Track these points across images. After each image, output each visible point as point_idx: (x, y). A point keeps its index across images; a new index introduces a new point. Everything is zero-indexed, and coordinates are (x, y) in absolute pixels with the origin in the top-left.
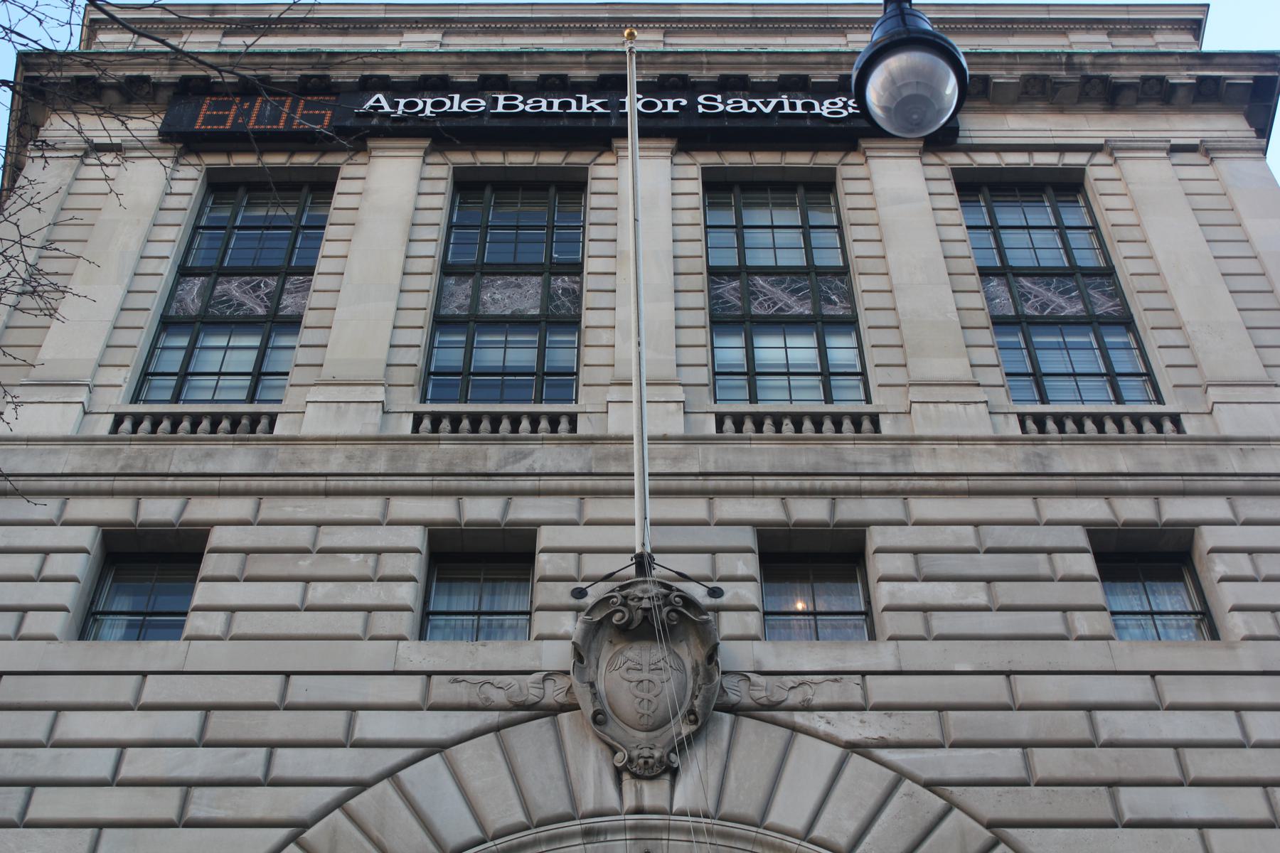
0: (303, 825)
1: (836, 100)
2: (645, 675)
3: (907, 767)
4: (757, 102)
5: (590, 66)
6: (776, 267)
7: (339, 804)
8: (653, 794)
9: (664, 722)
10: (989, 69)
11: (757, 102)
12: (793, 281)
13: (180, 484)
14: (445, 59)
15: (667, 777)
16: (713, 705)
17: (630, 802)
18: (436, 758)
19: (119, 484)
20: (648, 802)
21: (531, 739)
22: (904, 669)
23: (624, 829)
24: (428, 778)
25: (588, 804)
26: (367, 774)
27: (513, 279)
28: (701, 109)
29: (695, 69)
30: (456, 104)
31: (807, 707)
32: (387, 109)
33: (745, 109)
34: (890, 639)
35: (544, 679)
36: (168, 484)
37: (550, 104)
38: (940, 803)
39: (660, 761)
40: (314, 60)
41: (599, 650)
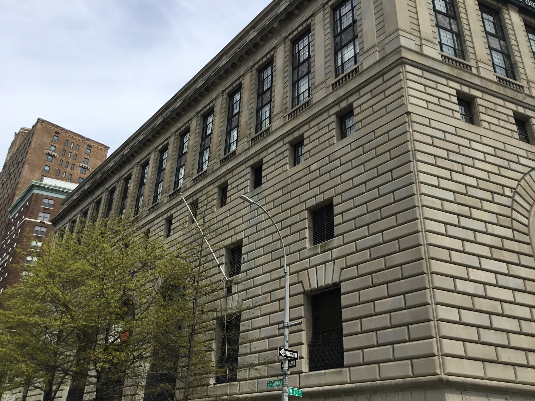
13: (468, 83)
19: (456, 79)
26: (526, 172)
36: (465, 83)
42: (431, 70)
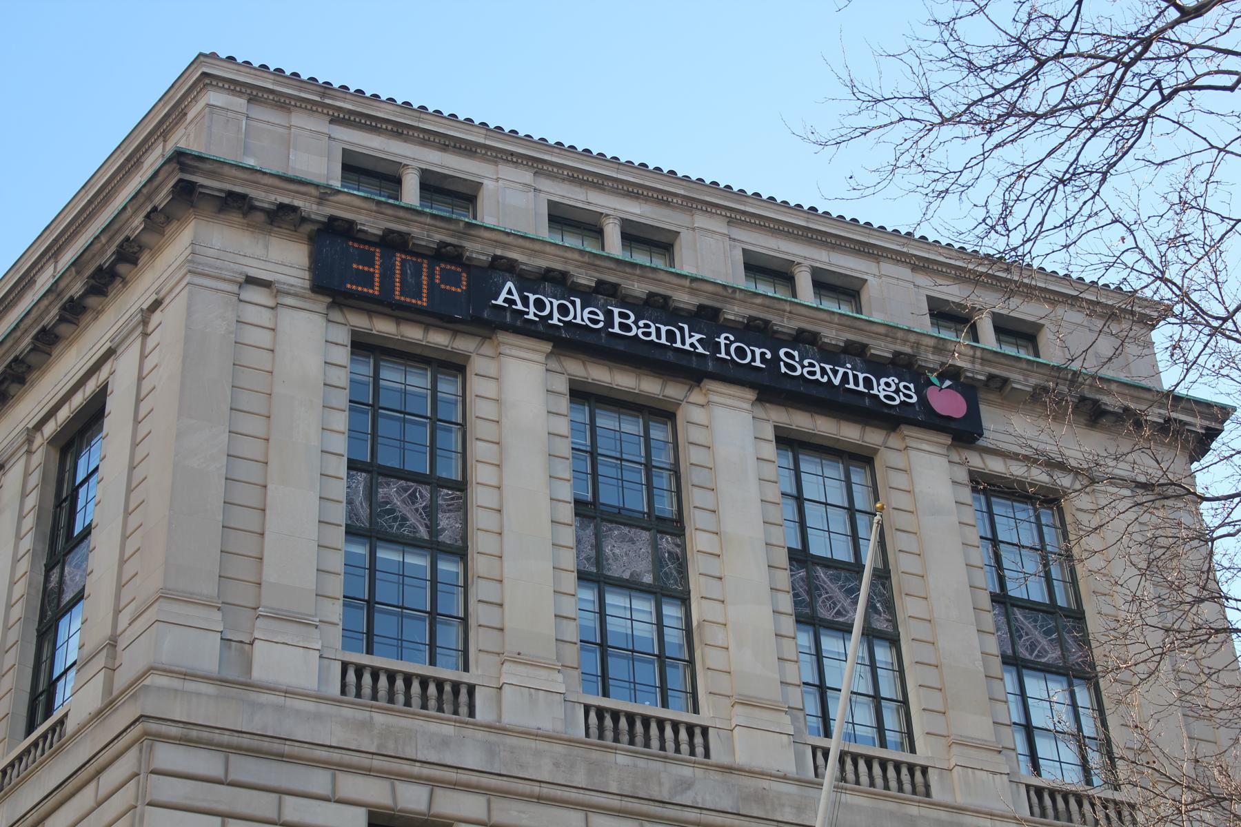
1: (890, 380)
4: (828, 367)
5: (693, 292)
6: (832, 560)
10: (1010, 371)
11: (828, 367)
12: (847, 579)
13: (427, 771)
14: (569, 255)
19: (377, 763)
27: (626, 530)
28: (783, 370)
29: (778, 315)
30: (581, 315)
32: (520, 307)
33: (818, 376)
36: (416, 769)
37: (655, 332)
40: (452, 227)
42: (266, 745)
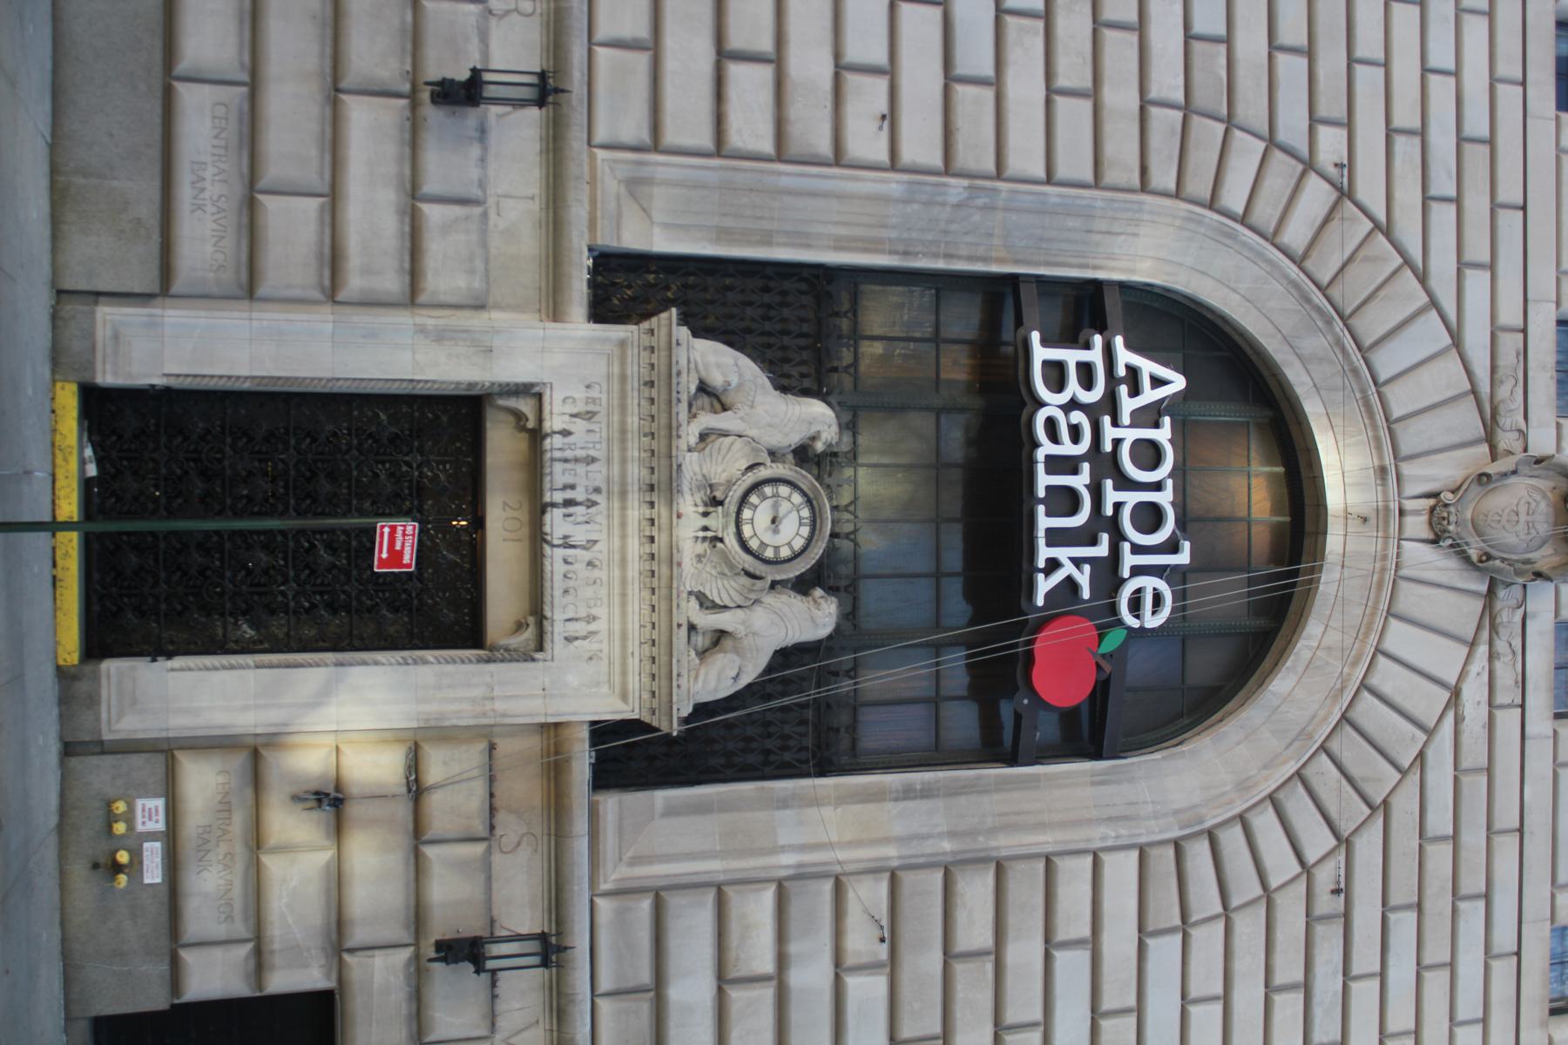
0: (1387, 231)
2: (1523, 518)
3: (1437, 738)
7: (1407, 262)
8: (1417, 525)
9: (1479, 533)
15: (1431, 536)
16: (1495, 575)
17: (1409, 505)
18: (1447, 340)
20: (1409, 520)
21: (1467, 420)
22: (1527, 743)
23: (1386, 500)
24: (1432, 334)
25: (1407, 469)
26: (1433, 283)
31: (1492, 657)
34: (1555, 732)
35: (1520, 431)
38: (1406, 764)
39: (1445, 531)
41: (1546, 478)
